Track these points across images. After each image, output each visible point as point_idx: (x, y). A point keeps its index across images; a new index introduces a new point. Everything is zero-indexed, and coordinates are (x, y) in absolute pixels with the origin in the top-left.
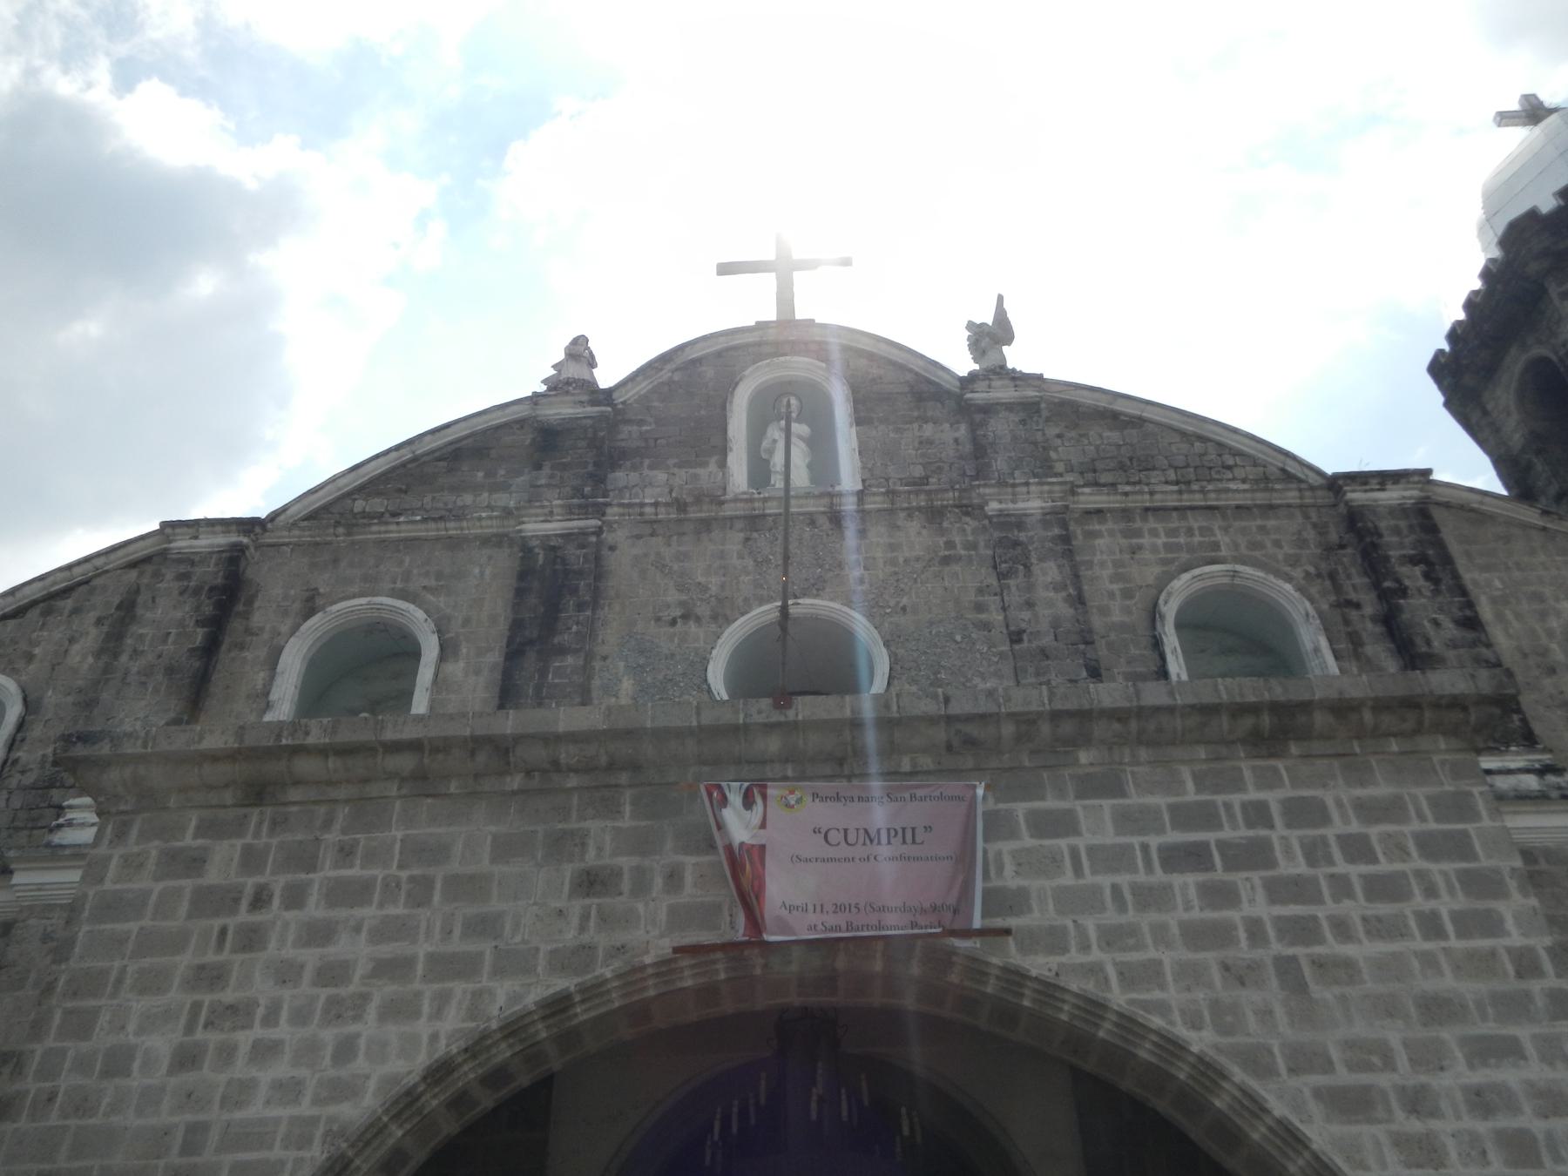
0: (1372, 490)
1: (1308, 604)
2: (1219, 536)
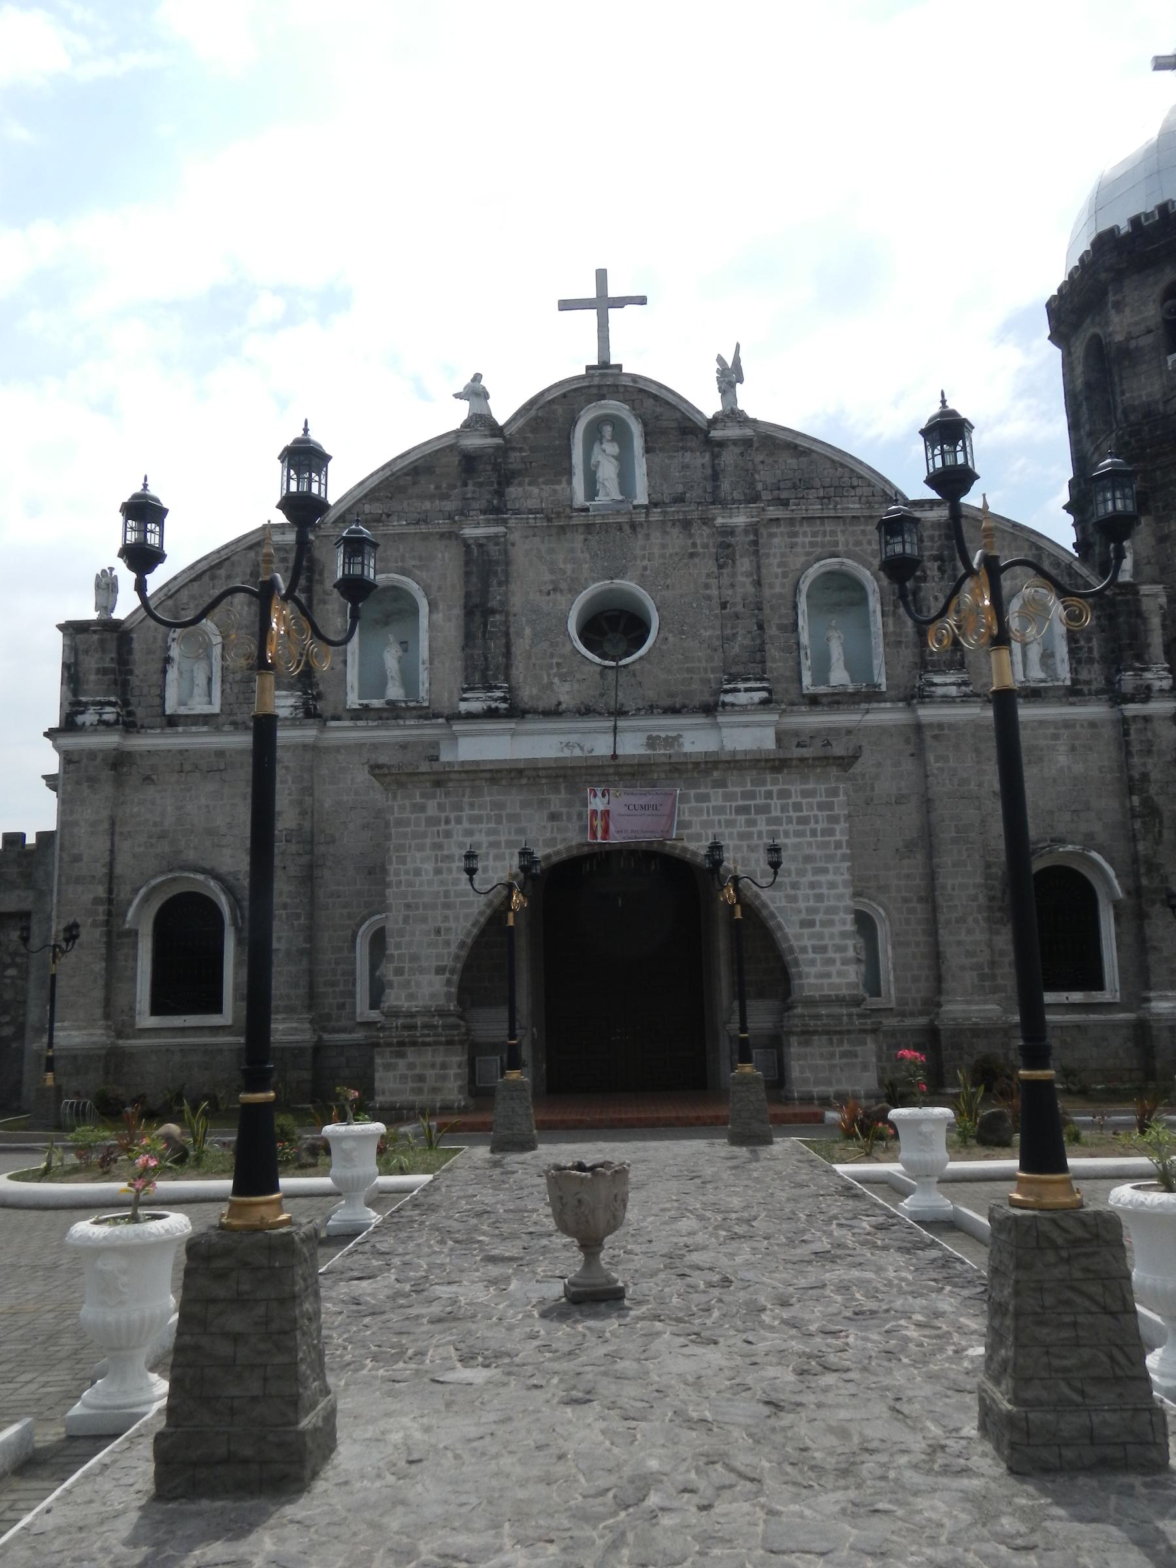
2: (841, 538)
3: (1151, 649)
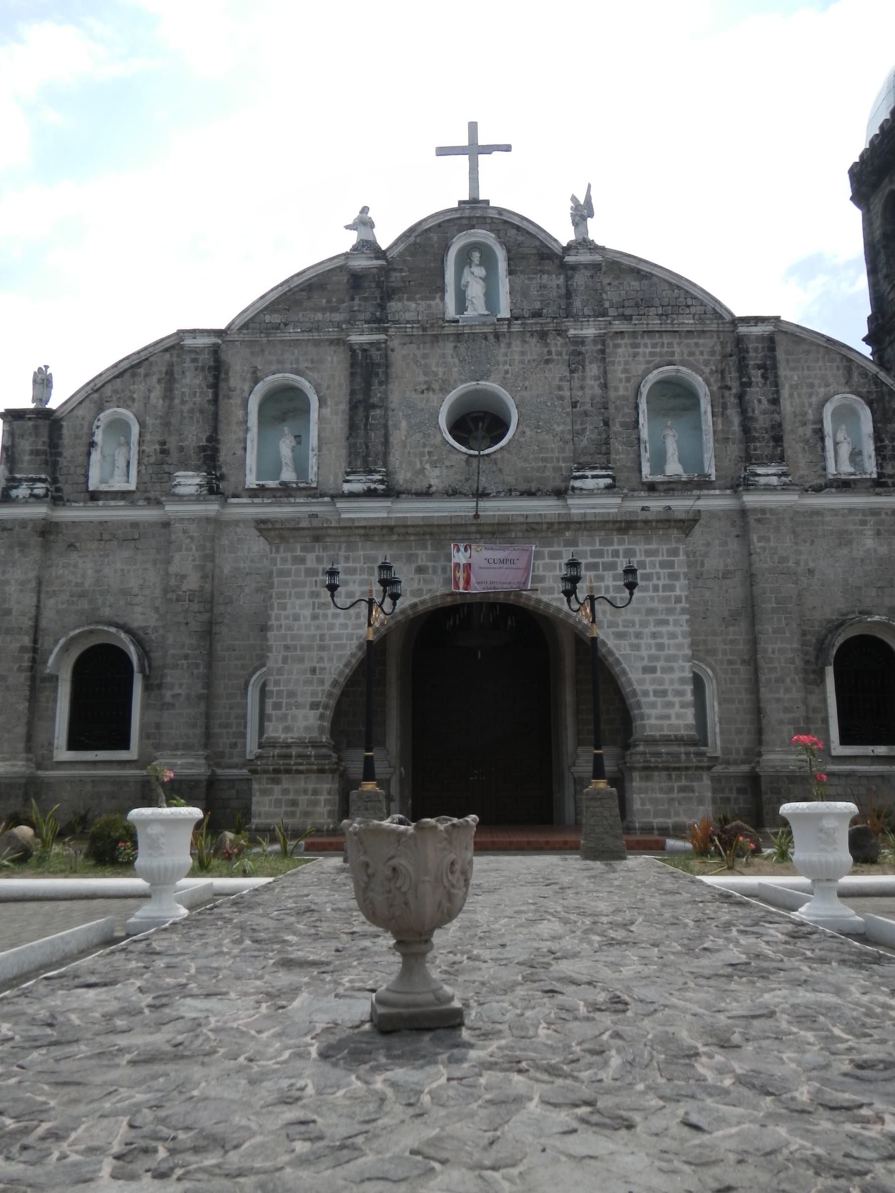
2: (677, 349)
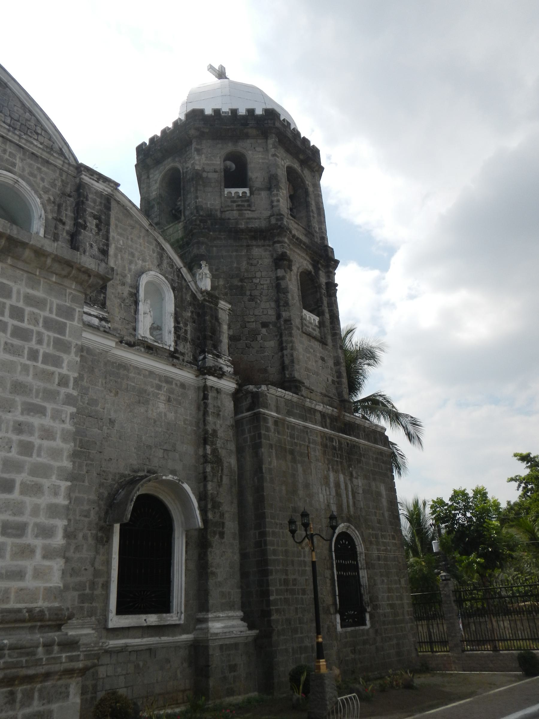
0: (93, 180)
1: (43, 212)
3: (222, 344)
